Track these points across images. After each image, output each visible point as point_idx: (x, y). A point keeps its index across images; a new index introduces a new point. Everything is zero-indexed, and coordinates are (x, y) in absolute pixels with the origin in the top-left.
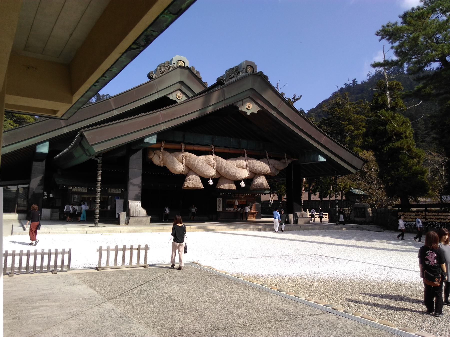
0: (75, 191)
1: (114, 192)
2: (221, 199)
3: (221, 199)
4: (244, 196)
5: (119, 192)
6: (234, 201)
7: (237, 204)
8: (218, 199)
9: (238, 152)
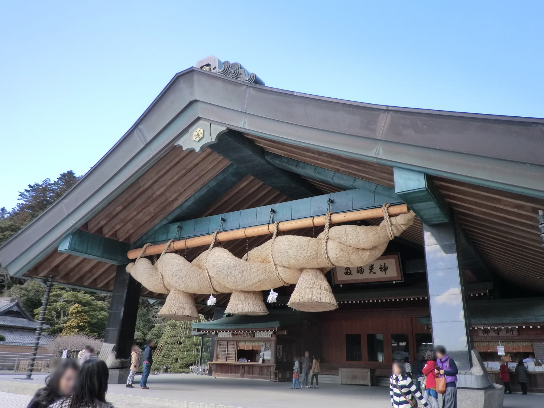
0: (220, 337)
1: (263, 336)
5: (268, 335)
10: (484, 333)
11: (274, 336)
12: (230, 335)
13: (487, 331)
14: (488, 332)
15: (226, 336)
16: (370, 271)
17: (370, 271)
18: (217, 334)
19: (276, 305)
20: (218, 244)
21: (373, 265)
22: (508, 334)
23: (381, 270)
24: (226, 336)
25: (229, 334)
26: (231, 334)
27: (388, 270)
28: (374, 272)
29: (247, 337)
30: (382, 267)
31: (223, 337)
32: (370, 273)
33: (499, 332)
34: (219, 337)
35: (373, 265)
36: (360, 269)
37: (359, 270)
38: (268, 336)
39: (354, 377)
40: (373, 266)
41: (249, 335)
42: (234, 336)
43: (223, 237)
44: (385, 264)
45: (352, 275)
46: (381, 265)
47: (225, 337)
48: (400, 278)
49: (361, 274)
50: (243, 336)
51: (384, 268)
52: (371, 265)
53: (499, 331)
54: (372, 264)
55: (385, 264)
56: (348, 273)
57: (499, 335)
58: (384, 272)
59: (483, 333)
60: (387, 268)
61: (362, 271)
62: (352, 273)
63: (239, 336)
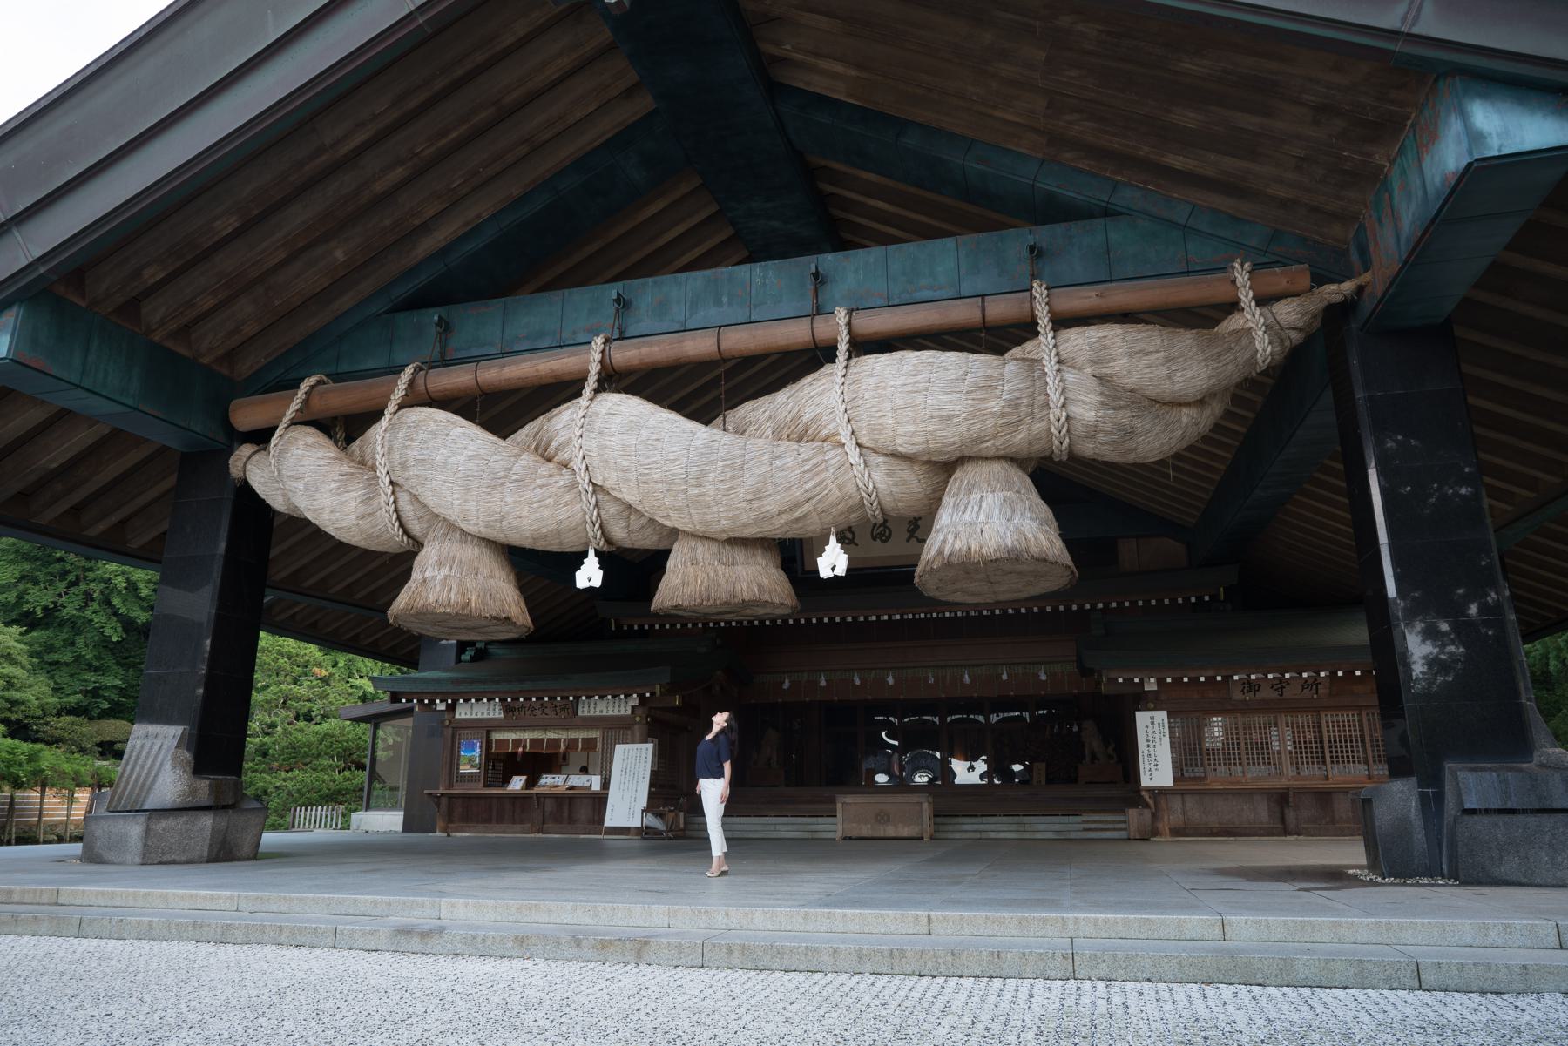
0: (463, 716)
1: (604, 713)
2: (1161, 715)
3: (1161, 715)
5: (623, 709)
8: (1142, 718)
9: (794, 333)
10: (1245, 691)
11: (640, 711)
12: (497, 711)
13: (1255, 686)
14: (1257, 688)
15: (483, 714)
16: (909, 534)
17: (909, 534)
18: (452, 708)
19: (625, 628)
20: (612, 380)
24: (483, 714)
25: (491, 709)
26: (497, 708)
29: (552, 715)
31: (474, 716)
32: (908, 540)
33: (1282, 687)
34: (457, 716)
35: (920, 518)
36: (882, 528)
37: (879, 531)
38: (622, 713)
39: (882, 818)
40: (919, 523)
41: (562, 709)
42: (511, 713)
43: (627, 354)
45: (857, 545)
47: (479, 716)
49: (884, 542)
50: (539, 712)
53: (1284, 684)
56: (847, 541)
57: (1281, 695)
59: (1243, 691)
61: (887, 534)
62: (856, 541)
63: (528, 713)
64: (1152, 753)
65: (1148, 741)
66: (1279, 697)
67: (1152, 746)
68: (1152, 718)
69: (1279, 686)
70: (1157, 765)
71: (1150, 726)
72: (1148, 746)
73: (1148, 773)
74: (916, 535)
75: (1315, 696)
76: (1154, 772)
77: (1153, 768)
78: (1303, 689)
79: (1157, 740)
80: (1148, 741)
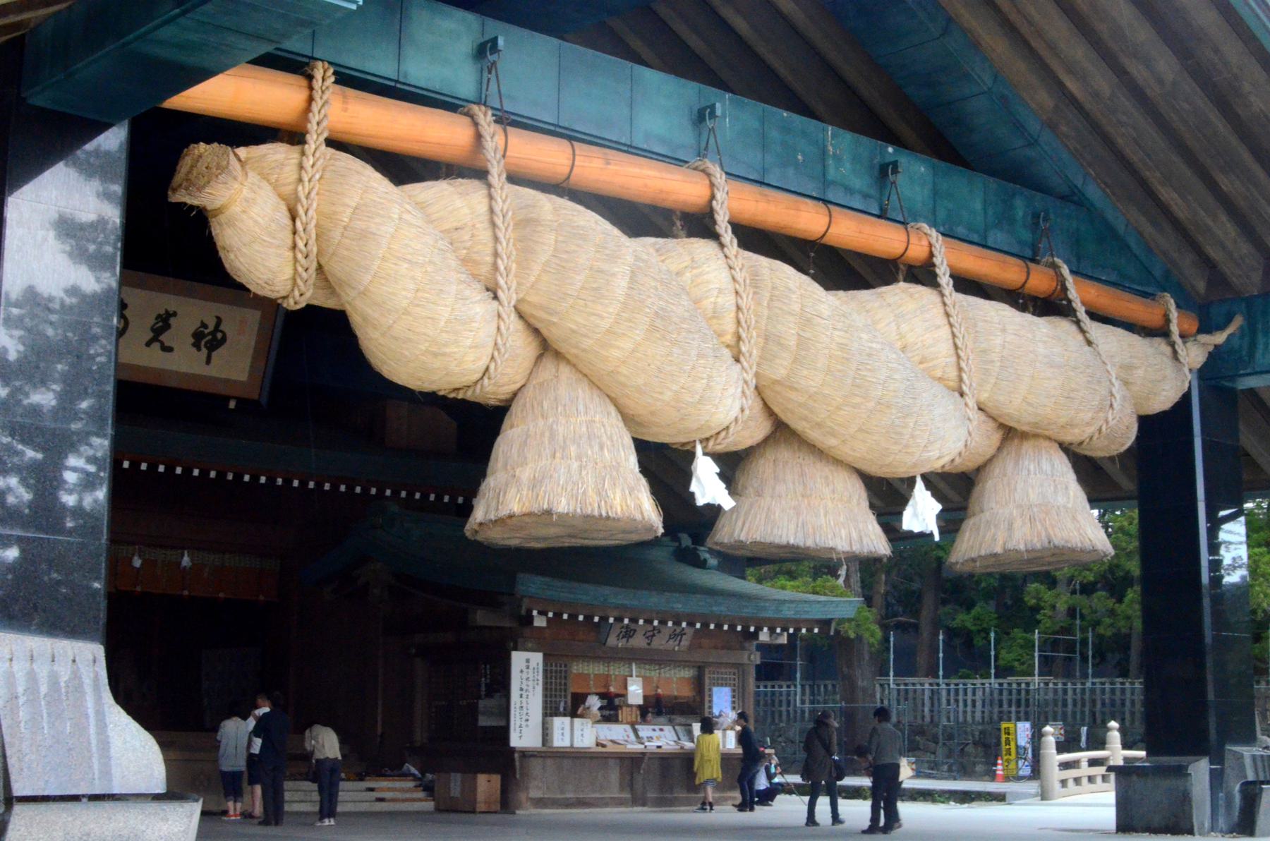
2: (537, 658)
3: (537, 658)
4: (685, 642)
6: (616, 670)
7: (636, 692)
10: (621, 636)
16: (151, 335)
17: (151, 335)
21: (175, 314)
22: (671, 642)
23: (197, 345)
27: (220, 350)
28: (167, 344)
30: (206, 331)
32: (148, 344)
33: (654, 635)
35: (175, 314)
40: (172, 321)
44: (219, 320)
46: (202, 322)
48: (255, 395)
51: (210, 337)
52: (162, 312)
54: (171, 309)
55: (219, 320)
57: (649, 644)
58: (204, 351)
59: (618, 636)
60: (224, 339)
64: (524, 705)
65: (522, 689)
66: (647, 647)
67: (524, 696)
68: (528, 661)
69: (651, 633)
70: (527, 720)
71: (525, 670)
72: (521, 696)
73: (518, 730)
74: (162, 338)
75: (677, 648)
76: (524, 729)
77: (524, 723)
78: (670, 638)
79: (530, 688)
80: (522, 689)
